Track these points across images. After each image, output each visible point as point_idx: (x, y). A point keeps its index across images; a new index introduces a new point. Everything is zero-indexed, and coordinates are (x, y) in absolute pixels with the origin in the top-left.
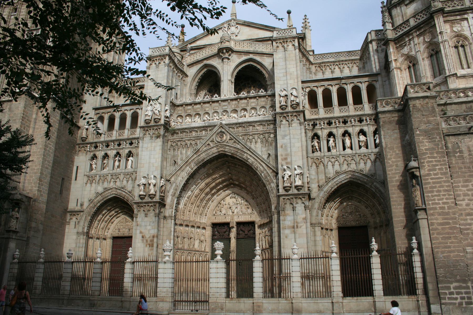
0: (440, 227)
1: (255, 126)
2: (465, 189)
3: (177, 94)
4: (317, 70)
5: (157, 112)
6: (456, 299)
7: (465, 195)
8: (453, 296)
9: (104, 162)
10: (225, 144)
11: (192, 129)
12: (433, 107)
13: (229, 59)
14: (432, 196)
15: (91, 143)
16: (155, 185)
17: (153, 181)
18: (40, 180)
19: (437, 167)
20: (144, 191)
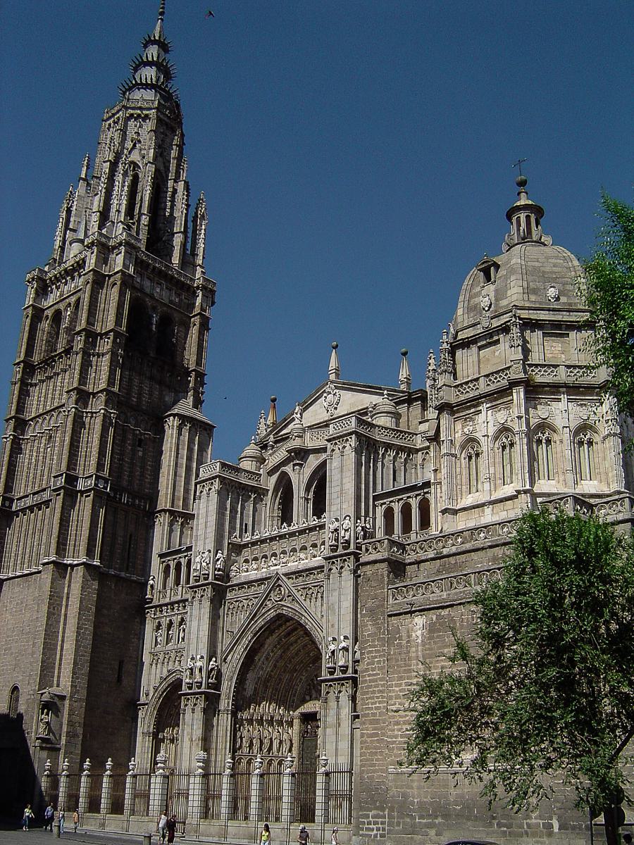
0: (369, 740)
1: (315, 574)
2: (397, 689)
3: (246, 524)
4: (424, 459)
5: (204, 564)
6: (373, 830)
7: (397, 697)
8: (370, 826)
9: (170, 633)
10: (282, 603)
11: (250, 583)
12: (382, 575)
13: (301, 465)
14: (367, 699)
15: (155, 607)
16: (200, 670)
17: (199, 664)
18: (74, 673)
19: (376, 660)
20: (190, 678)
